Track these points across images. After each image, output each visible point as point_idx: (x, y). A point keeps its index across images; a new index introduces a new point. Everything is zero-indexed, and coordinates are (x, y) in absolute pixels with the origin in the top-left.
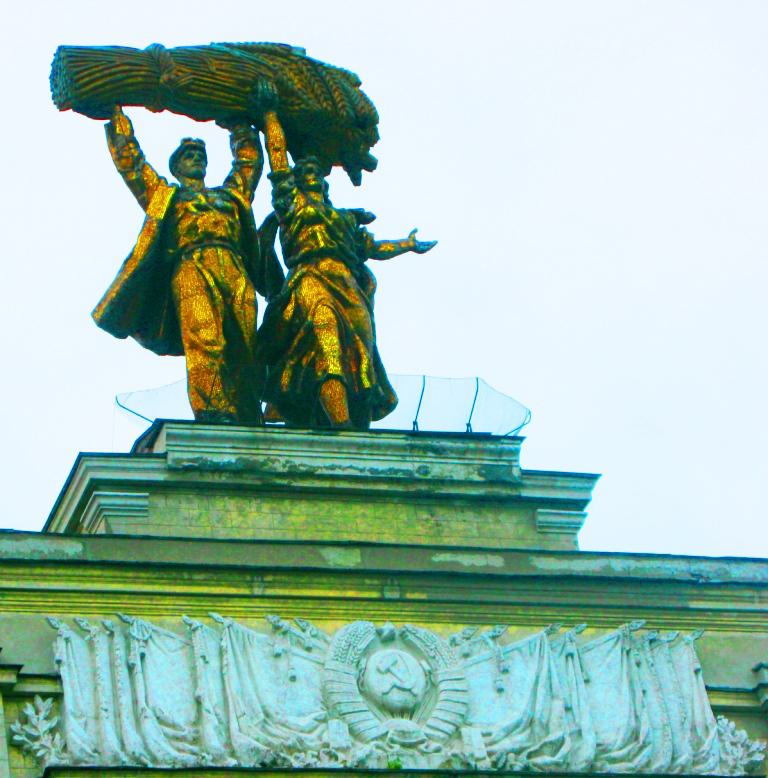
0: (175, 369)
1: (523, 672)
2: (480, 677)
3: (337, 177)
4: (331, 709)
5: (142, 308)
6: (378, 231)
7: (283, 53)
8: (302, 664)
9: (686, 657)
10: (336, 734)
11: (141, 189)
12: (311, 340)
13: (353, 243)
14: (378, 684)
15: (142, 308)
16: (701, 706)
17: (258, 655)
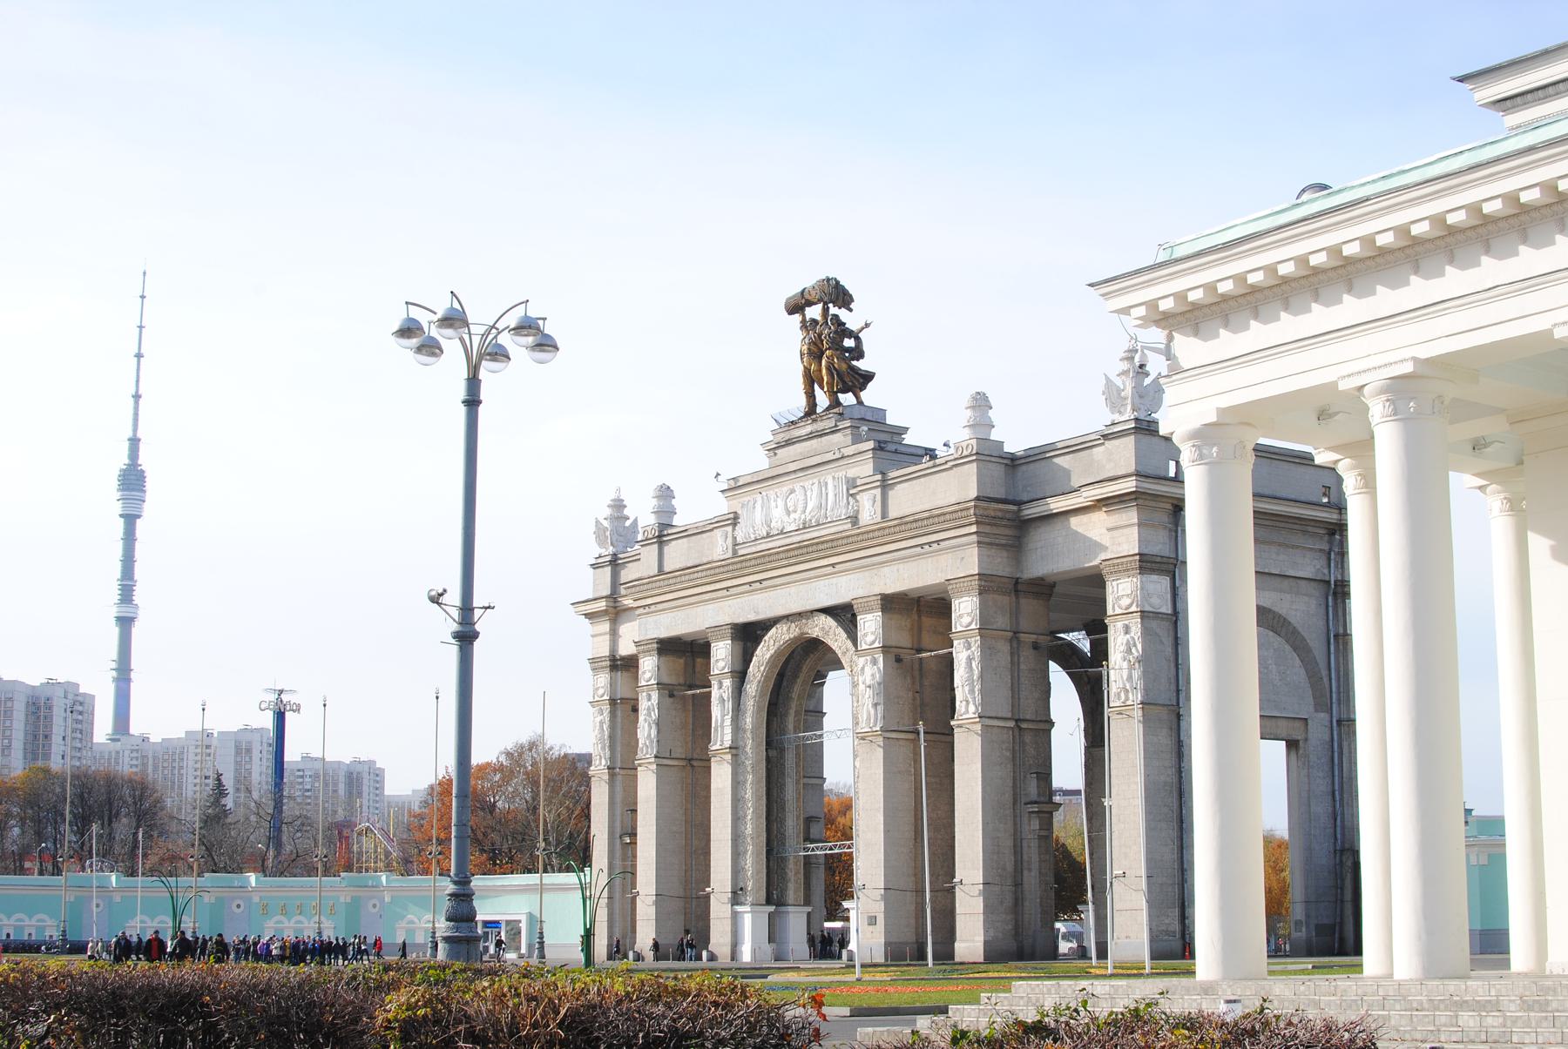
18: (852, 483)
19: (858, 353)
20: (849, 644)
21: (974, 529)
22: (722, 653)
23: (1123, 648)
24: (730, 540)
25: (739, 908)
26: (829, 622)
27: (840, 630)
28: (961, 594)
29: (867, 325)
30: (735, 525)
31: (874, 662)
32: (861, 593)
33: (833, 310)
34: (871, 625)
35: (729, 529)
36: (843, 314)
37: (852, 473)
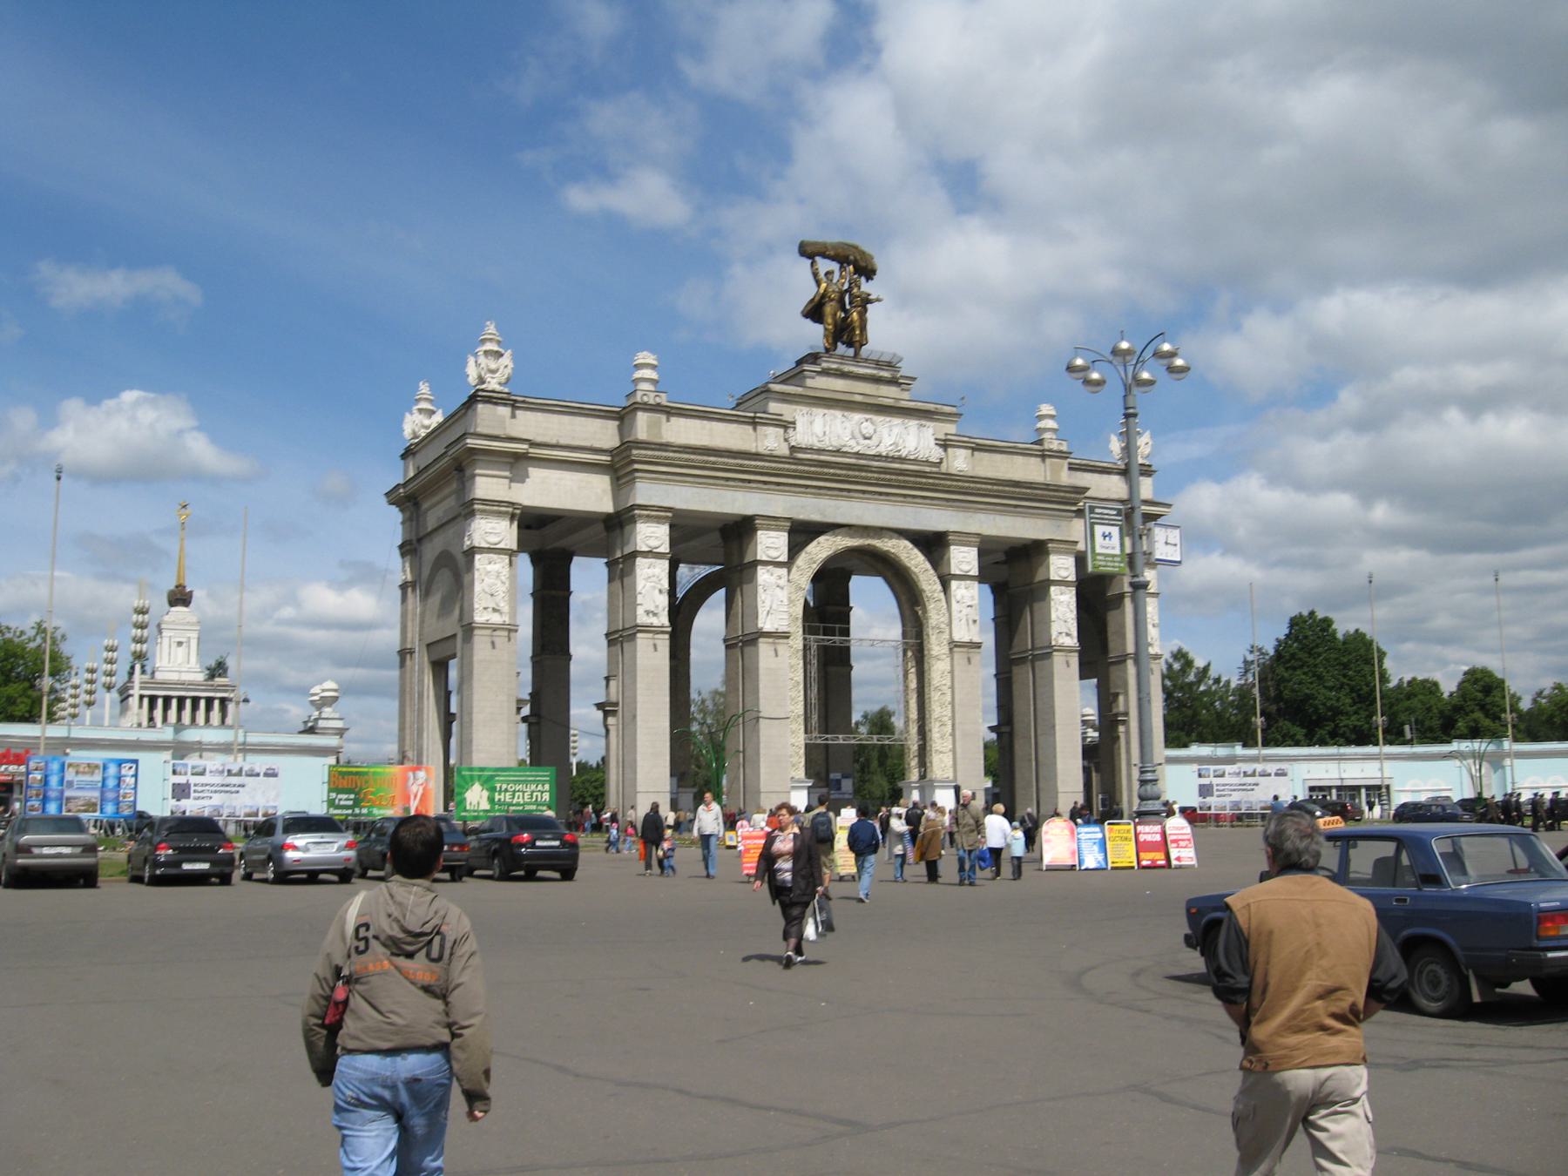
0: (819, 328)
1: (896, 430)
2: (885, 432)
3: (863, 279)
4: (853, 437)
5: (814, 312)
7: (856, 248)
8: (847, 424)
9: (931, 431)
10: (853, 443)
11: (818, 283)
12: (854, 329)
13: (866, 301)
15: (814, 312)
16: (933, 442)
17: (838, 421)
20: (928, 565)
22: (771, 543)
27: (916, 551)
28: (1059, 552)
29: (878, 300)
32: (952, 528)
34: (964, 559)
36: (866, 287)
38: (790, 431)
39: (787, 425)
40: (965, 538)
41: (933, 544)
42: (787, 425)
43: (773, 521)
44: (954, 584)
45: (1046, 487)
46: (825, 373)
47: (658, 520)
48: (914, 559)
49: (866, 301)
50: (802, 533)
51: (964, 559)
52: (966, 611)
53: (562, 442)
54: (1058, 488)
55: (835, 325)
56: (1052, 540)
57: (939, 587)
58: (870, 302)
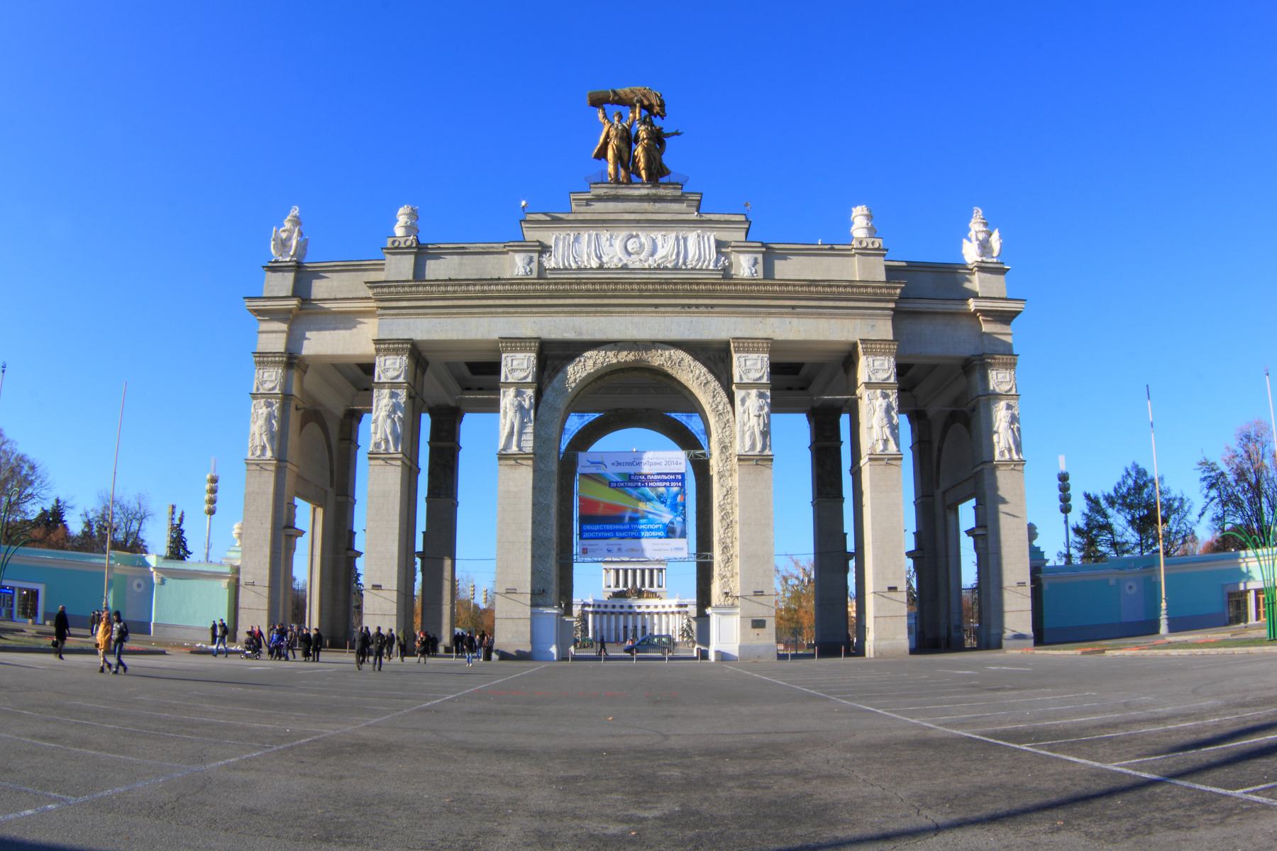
6: (665, 131)
14: (629, 248)
18: (720, 244)
19: (661, 151)
20: (710, 377)
21: (892, 305)
23: (1008, 419)
24: (535, 265)
25: (536, 609)
26: (680, 354)
29: (677, 134)
30: (541, 253)
31: (761, 396)
32: (739, 334)
33: (645, 113)
35: (535, 256)
36: (657, 122)
37: (725, 236)
38: (546, 257)
39: (544, 249)
40: (749, 345)
41: (716, 357)
42: (544, 249)
43: (517, 343)
44: (739, 394)
45: (851, 284)
46: (599, 199)
47: (396, 352)
48: (692, 375)
49: (658, 139)
50: (553, 356)
51: (750, 367)
52: (754, 421)
53: (339, 296)
54: (865, 284)
55: (619, 158)
56: (863, 341)
57: (726, 400)
58: (668, 135)
